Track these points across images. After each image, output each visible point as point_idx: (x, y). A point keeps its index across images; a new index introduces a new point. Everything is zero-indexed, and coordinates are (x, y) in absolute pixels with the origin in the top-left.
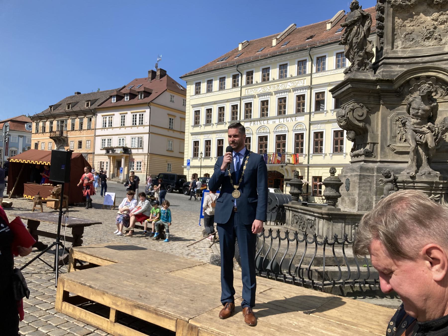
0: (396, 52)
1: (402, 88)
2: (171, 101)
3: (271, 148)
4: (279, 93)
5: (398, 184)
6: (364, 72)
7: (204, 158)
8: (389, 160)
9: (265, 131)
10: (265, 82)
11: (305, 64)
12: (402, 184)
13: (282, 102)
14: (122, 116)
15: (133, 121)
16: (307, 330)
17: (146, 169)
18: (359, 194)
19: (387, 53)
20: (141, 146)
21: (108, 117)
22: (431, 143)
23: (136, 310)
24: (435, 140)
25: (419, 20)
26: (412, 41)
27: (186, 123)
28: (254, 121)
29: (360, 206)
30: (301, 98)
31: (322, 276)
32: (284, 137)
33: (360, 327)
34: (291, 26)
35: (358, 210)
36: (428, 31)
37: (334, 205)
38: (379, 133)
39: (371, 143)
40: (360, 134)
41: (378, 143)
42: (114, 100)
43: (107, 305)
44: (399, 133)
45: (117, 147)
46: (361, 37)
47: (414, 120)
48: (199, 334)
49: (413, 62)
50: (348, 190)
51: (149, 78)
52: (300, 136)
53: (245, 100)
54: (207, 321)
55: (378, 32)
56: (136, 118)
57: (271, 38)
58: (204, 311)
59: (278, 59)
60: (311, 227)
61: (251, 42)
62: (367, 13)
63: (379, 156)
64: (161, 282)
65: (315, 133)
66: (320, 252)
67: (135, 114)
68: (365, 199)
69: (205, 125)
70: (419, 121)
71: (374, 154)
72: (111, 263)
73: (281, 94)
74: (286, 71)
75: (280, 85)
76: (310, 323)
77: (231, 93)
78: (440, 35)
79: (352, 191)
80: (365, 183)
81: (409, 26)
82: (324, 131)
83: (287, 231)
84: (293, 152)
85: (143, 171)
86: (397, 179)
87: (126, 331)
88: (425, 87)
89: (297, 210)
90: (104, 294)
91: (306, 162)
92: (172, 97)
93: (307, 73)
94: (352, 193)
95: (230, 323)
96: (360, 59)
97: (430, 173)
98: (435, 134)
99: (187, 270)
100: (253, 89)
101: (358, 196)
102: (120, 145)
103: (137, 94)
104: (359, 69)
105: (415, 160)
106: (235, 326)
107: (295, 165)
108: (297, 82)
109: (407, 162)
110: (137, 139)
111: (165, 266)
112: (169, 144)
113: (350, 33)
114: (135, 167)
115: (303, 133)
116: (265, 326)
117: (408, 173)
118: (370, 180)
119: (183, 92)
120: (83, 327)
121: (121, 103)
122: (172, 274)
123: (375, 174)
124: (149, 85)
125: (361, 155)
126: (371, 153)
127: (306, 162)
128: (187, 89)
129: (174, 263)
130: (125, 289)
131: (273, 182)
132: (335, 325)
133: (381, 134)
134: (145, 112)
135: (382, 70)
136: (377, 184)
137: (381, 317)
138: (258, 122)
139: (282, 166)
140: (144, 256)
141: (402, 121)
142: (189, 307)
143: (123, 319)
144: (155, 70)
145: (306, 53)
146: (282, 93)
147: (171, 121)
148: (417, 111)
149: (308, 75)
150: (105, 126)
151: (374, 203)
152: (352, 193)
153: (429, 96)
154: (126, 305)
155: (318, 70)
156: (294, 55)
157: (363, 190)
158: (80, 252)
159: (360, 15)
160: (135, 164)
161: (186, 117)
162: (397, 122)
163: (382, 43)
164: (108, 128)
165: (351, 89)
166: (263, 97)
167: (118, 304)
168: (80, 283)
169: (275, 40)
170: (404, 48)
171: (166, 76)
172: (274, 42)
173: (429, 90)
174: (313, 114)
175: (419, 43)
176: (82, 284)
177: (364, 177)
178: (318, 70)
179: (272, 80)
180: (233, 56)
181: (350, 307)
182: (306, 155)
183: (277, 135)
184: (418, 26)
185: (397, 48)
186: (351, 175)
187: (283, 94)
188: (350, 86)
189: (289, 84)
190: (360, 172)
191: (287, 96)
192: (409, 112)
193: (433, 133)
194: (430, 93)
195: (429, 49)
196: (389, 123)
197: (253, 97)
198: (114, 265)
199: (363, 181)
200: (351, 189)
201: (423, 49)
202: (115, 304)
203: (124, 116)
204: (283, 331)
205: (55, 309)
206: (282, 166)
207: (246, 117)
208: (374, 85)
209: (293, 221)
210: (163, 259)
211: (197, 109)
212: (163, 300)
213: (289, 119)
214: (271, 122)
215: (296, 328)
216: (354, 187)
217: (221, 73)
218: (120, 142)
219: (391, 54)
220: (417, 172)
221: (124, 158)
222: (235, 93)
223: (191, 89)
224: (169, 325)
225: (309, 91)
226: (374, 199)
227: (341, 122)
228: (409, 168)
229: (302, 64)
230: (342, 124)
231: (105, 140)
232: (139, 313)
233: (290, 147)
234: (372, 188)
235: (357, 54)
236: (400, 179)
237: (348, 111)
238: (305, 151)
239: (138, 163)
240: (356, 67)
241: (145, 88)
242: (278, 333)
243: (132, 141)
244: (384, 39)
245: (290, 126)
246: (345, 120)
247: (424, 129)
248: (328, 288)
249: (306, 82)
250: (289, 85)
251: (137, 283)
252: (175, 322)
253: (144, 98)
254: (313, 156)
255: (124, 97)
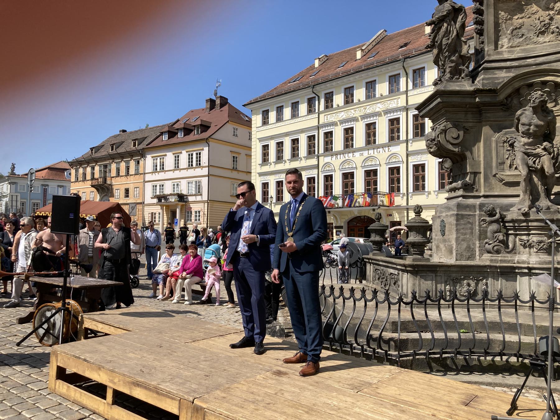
0: (501, 53)
1: (509, 99)
2: (234, 135)
3: (359, 186)
4: (367, 118)
5: (507, 224)
6: (459, 82)
7: (276, 204)
8: (496, 194)
9: (350, 166)
10: (348, 105)
11: (399, 81)
12: (511, 224)
13: (371, 129)
14: (175, 157)
15: (189, 162)
16: (348, 412)
17: (206, 220)
18: (457, 239)
19: (489, 55)
20: (199, 192)
21: (159, 158)
22: (548, 168)
23: (134, 388)
24: (554, 164)
25: (530, 10)
26: (522, 37)
27: (253, 161)
28: (337, 154)
29: (459, 255)
30: (395, 122)
31: (401, 345)
32: (375, 172)
33: (420, 409)
34: (379, 33)
35: (456, 260)
36: (543, 23)
37: (422, 253)
38: (482, 159)
39: (471, 173)
40: (458, 162)
41: (480, 173)
42: (165, 137)
43: (104, 383)
44: (507, 158)
45: (171, 195)
46: (453, 37)
47: (525, 140)
48: (206, 417)
49: (523, 64)
50: (443, 235)
51: (207, 108)
52: (395, 171)
53: (324, 129)
54: (217, 401)
55: (476, 29)
56: (192, 159)
57: (355, 50)
58: (217, 389)
59: (363, 74)
60: (395, 284)
61: (330, 56)
62: (460, 5)
63: (482, 190)
64: (176, 354)
65: (414, 166)
66: (394, 314)
67: (190, 153)
68: (464, 245)
69: (276, 163)
70: (531, 140)
71: (476, 186)
72: (125, 332)
73: (369, 119)
74: (375, 90)
75: (368, 107)
76: (355, 404)
77: (306, 121)
78: (557, 28)
79: (449, 235)
80: (465, 224)
81: (517, 20)
82: (426, 163)
83: (363, 288)
84: (388, 192)
85: (202, 223)
86: (505, 217)
87: (124, 416)
88: (536, 95)
89: (378, 262)
90: (100, 369)
91: (404, 204)
92: (235, 130)
93: (401, 90)
94: (449, 239)
95: (246, 403)
96: (453, 65)
97: (548, 208)
98: (554, 156)
99: (216, 339)
100: (334, 115)
101: (456, 242)
102: (174, 191)
103: (193, 128)
104: (452, 78)
105: (528, 192)
106: (252, 406)
107: (391, 208)
108: (389, 102)
109: (518, 196)
110: (194, 183)
111: (189, 335)
112: (233, 187)
113: (438, 32)
114: (193, 218)
115: (399, 167)
116: (292, 407)
117: (519, 210)
118: (471, 221)
119: (248, 123)
120: (77, 411)
121: (174, 140)
122: (195, 344)
123: (478, 212)
124: (207, 117)
125: (458, 189)
126: (472, 185)
127: (404, 204)
128: (253, 119)
129: (202, 330)
130: (127, 362)
131: (364, 230)
132: (388, 407)
133: (484, 160)
134: (203, 150)
135: (482, 77)
136: (480, 226)
137: (453, 395)
138: (342, 156)
139: (374, 210)
140: (167, 323)
141: (509, 141)
142: (200, 384)
143: (122, 400)
144: (214, 98)
145: (398, 65)
146: (370, 117)
147: (235, 159)
148: (527, 127)
149: (402, 93)
150: (156, 169)
151: (477, 250)
152: (449, 239)
153: (543, 106)
154: (124, 383)
155: (415, 86)
156: (384, 69)
157: (462, 234)
158: (90, 319)
159: (450, 8)
160: (193, 213)
161: (253, 154)
162: (505, 144)
163: (483, 43)
164: (159, 172)
165: (441, 104)
166: (347, 124)
167: (116, 380)
168: (74, 356)
169: (360, 51)
170: (511, 47)
171: (227, 105)
172: (359, 55)
173: (541, 99)
174: (411, 142)
175: (530, 40)
176: (76, 357)
177: (463, 216)
178: (415, 86)
179: (357, 101)
180: (308, 75)
181: (418, 383)
182: (404, 194)
183: (365, 171)
184: (529, 17)
185: (501, 48)
186: (447, 215)
187: (372, 119)
188: (439, 100)
189: (379, 105)
190: (457, 211)
191: (377, 121)
192: (518, 130)
193: (552, 156)
194: (544, 103)
195: (544, 46)
196: (494, 145)
197: (334, 124)
198: (125, 333)
199: (462, 222)
200: (447, 233)
201: (536, 48)
202: (112, 381)
203: (178, 156)
204: (314, 413)
205: (48, 389)
206: (374, 210)
207: (326, 150)
208: (472, 97)
209: (375, 277)
210: (191, 326)
211: (265, 143)
212: (170, 375)
213: (381, 150)
214: (357, 154)
215: (333, 410)
216: (450, 231)
217: (293, 97)
218: (174, 188)
219: (493, 55)
220: (530, 208)
221: (180, 207)
222: (311, 121)
223: (257, 120)
224: (171, 407)
225: (405, 113)
226: (478, 245)
227: (431, 148)
228: (520, 203)
229: (394, 80)
230: (432, 150)
231: (156, 186)
232: (138, 392)
233: (383, 185)
234: (474, 231)
235: (449, 59)
236: (509, 217)
237: (438, 133)
238: (403, 189)
239: (196, 212)
240: (448, 75)
241: (201, 120)
242: (306, 415)
243: (189, 186)
244: (485, 38)
245: (381, 160)
246: (435, 144)
247: (539, 150)
248: (407, 360)
249: (401, 101)
250: (379, 107)
251: (145, 355)
252: (177, 402)
253: (201, 133)
254: (412, 195)
255: (177, 133)
